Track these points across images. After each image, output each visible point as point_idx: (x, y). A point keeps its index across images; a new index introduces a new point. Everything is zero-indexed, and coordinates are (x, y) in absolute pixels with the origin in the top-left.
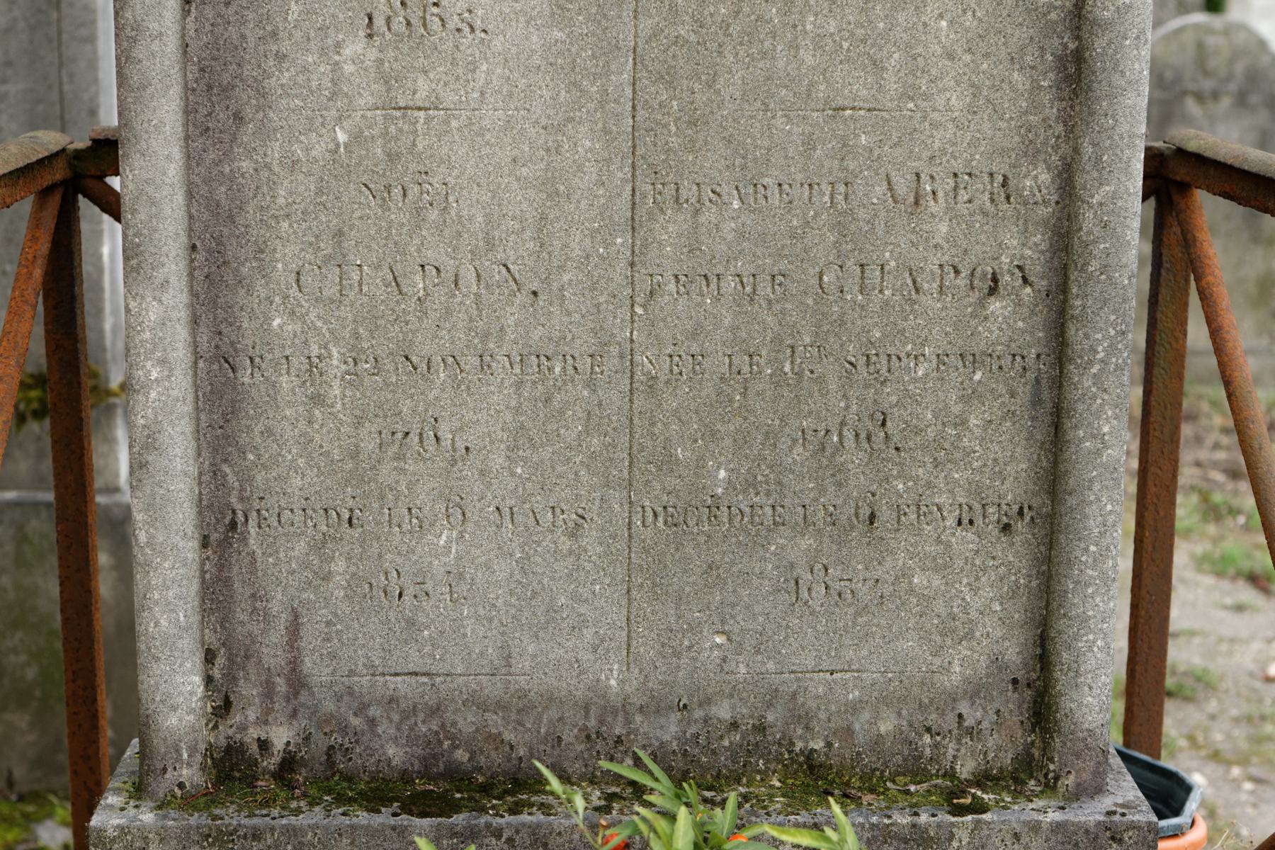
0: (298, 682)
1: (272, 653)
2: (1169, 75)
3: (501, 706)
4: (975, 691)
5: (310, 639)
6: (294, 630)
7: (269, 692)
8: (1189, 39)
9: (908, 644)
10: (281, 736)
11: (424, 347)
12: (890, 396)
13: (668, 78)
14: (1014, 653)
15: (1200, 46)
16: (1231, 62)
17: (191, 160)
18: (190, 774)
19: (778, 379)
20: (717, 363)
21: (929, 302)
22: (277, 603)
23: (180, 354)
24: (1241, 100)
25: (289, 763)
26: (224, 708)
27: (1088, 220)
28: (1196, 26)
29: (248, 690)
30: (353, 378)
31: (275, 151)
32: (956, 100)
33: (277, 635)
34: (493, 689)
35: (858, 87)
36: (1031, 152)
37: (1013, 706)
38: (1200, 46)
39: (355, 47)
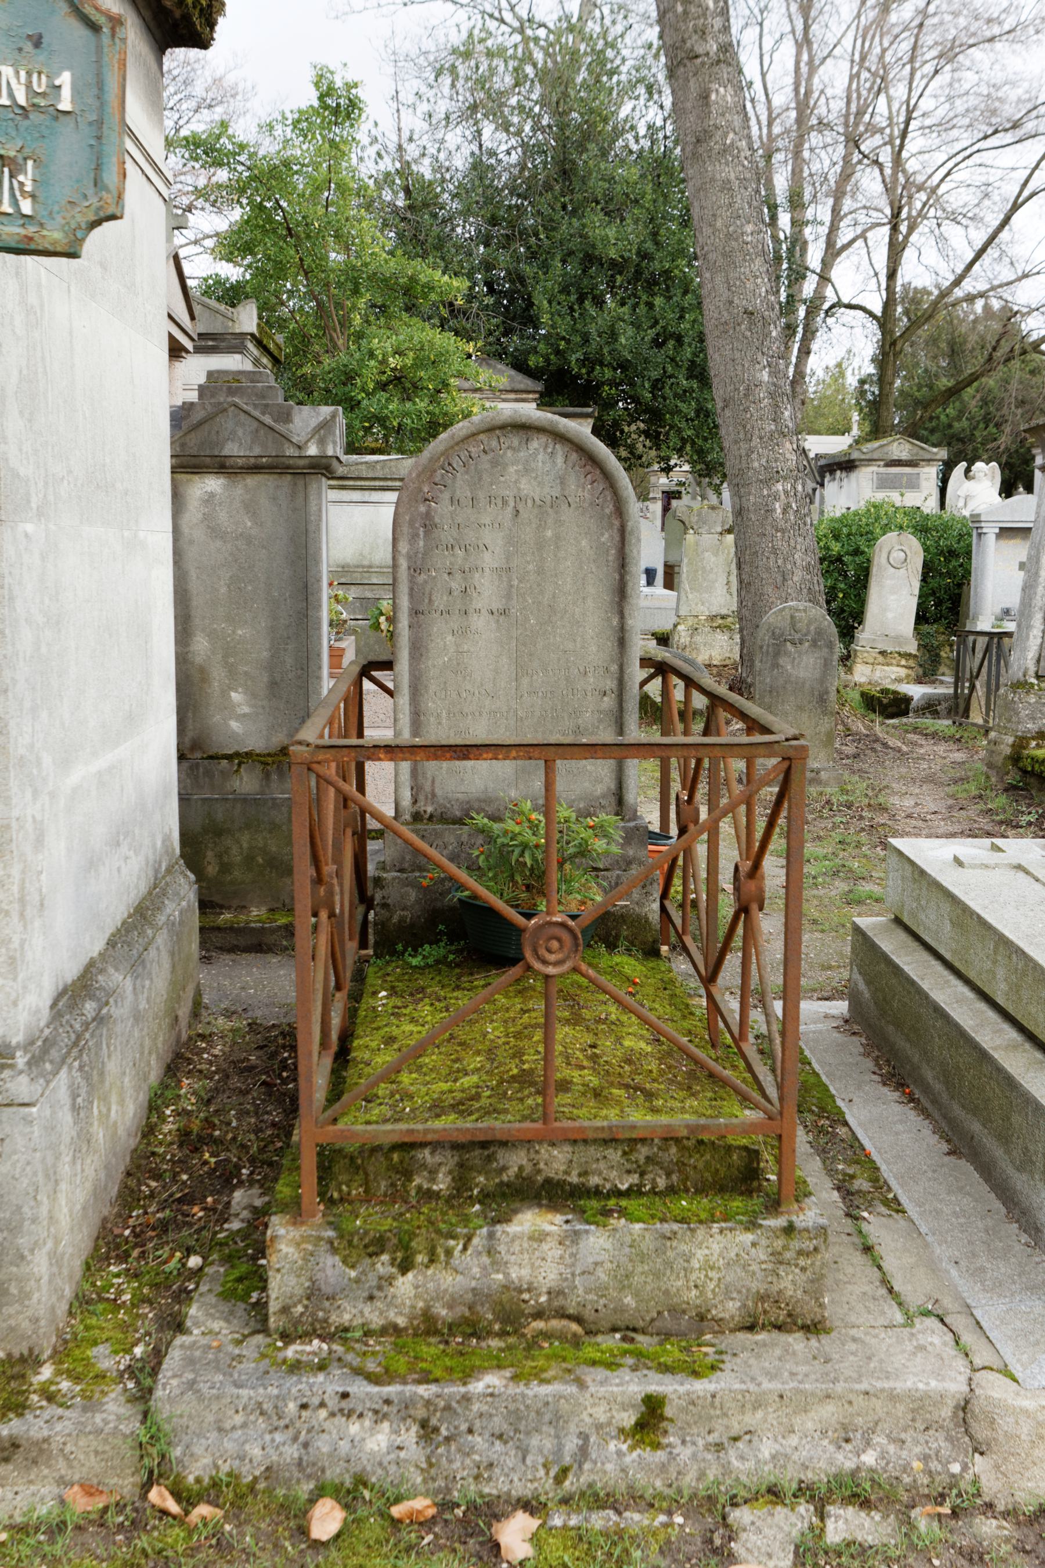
0: (434, 795)
1: (428, 787)
2: (777, 631)
3: (485, 801)
4: (604, 796)
5: (437, 784)
6: (433, 782)
7: (426, 798)
8: (787, 614)
9: (587, 784)
10: (430, 809)
11: (466, 710)
12: (580, 721)
13: (524, 644)
14: (613, 786)
15: (792, 617)
16: (808, 625)
17: (410, 665)
18: (407, 817)
19: (552, 717)
20: (537, 714)
21: (589, 698)
22: (429, 775)
23: (407, 712)
24: (814, 644)
25: (431, 816)
26: (415, 802)
27: (626, 677)
28: (790, 608)
29: (421, 797)
30: (449, 718)
31: (430, 663)
32: (594, 649)
33: (429, 783)
34: (483, 796)
35: (570, 646)
36: (612, 661)
37: (613, 800)
38: (792, 617)
39: (450, 638)
